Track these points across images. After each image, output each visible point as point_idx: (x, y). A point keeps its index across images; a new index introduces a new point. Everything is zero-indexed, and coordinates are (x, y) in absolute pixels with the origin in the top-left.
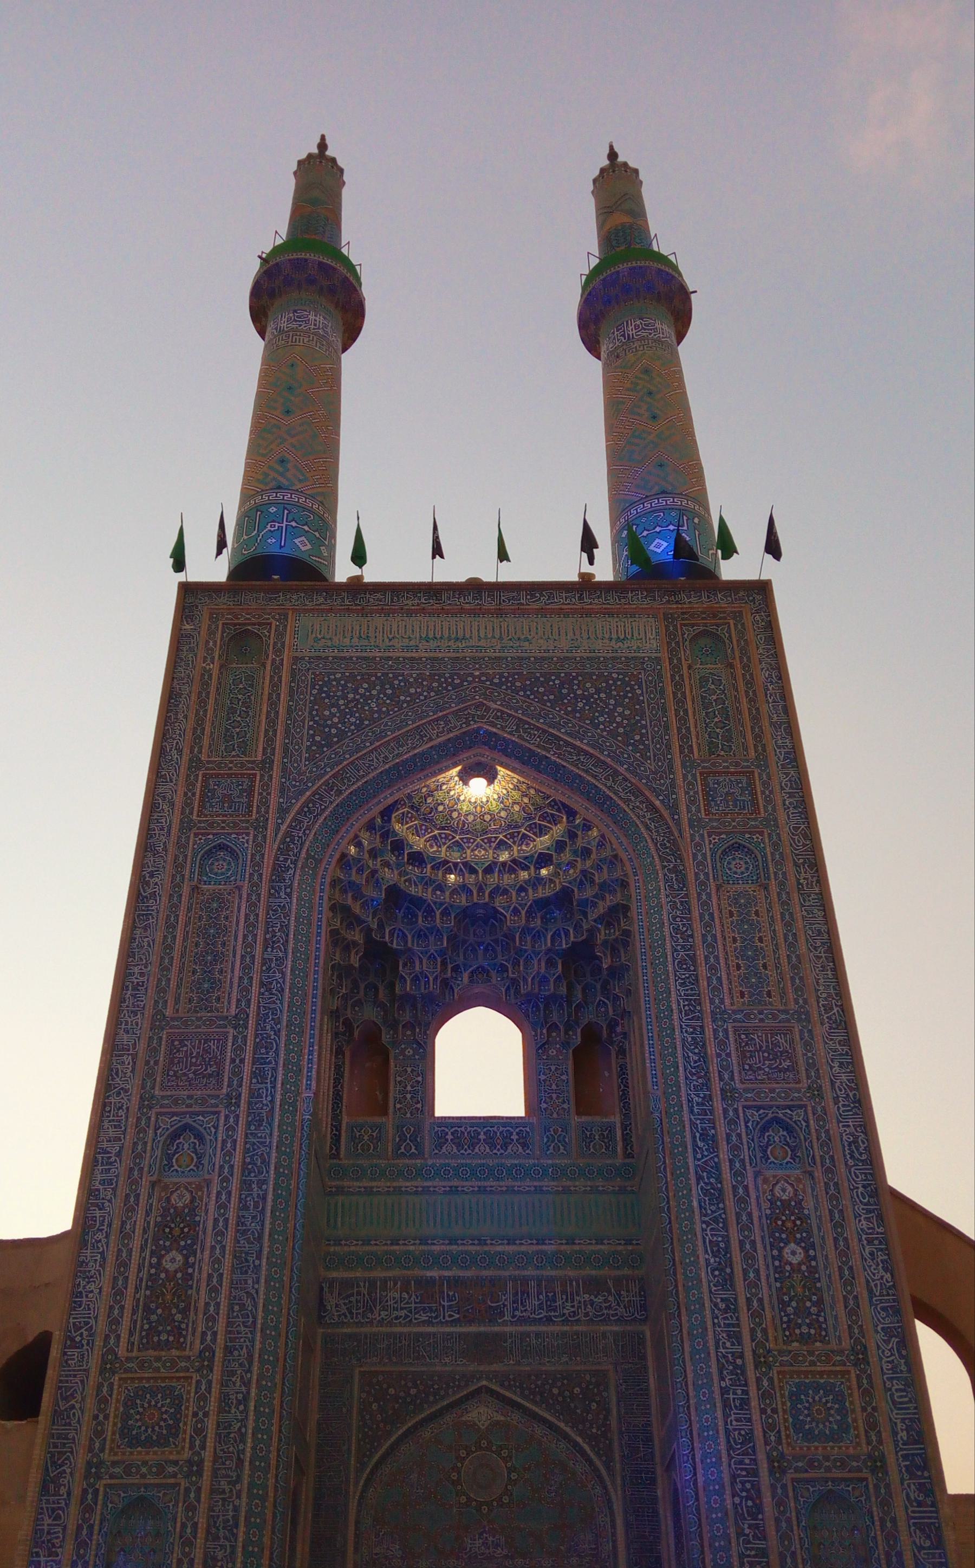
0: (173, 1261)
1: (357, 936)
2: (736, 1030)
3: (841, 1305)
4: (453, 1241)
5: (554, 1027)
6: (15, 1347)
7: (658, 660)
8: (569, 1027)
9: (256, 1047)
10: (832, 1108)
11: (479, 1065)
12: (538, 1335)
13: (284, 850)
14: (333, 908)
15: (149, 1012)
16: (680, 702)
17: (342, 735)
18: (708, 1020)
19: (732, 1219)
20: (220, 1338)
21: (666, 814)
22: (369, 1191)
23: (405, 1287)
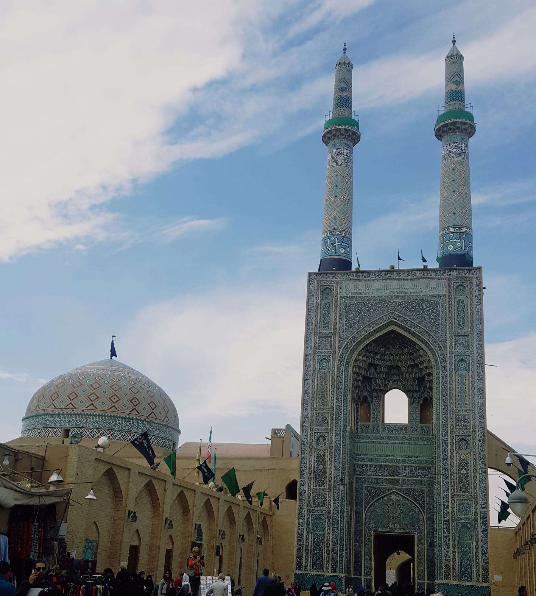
0: (321, 467)
1: (360, 378)
2: (456, 414)
3: (473, 485)
4: (387, 456)
5: (415, 398)
6: (289, 482)
7: (445, 295)
8: (419, 398)
9: (336, 415)
10: (477, 437)
11: (396, 407)
12: (408, 480)
13: (340, 360)
14: (354, 373)
15: (310, 406)
16: (450, 311)
17: (354, 323)
18: (449, 412)
19: (449, 464)
20: (332, 485)
21: (443, 349)
22: (366, 442)
23: (375, 467)
